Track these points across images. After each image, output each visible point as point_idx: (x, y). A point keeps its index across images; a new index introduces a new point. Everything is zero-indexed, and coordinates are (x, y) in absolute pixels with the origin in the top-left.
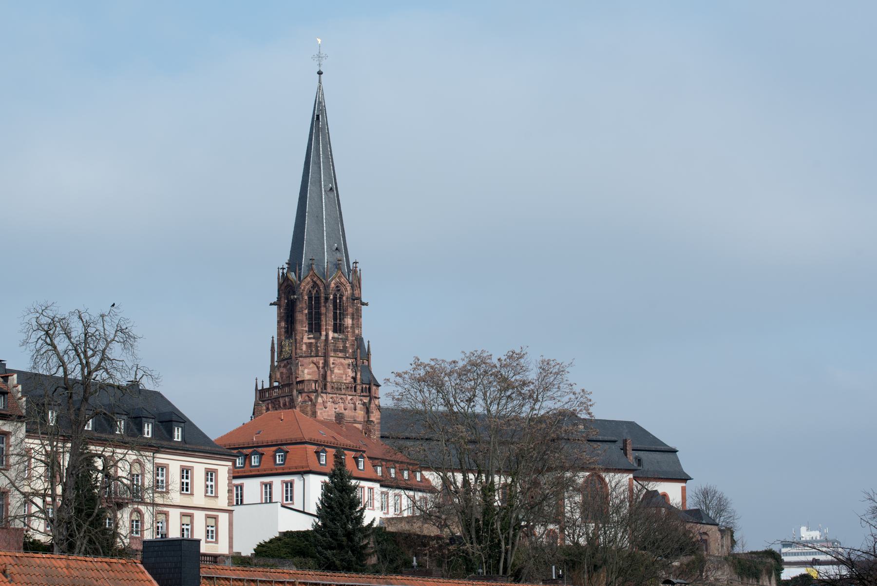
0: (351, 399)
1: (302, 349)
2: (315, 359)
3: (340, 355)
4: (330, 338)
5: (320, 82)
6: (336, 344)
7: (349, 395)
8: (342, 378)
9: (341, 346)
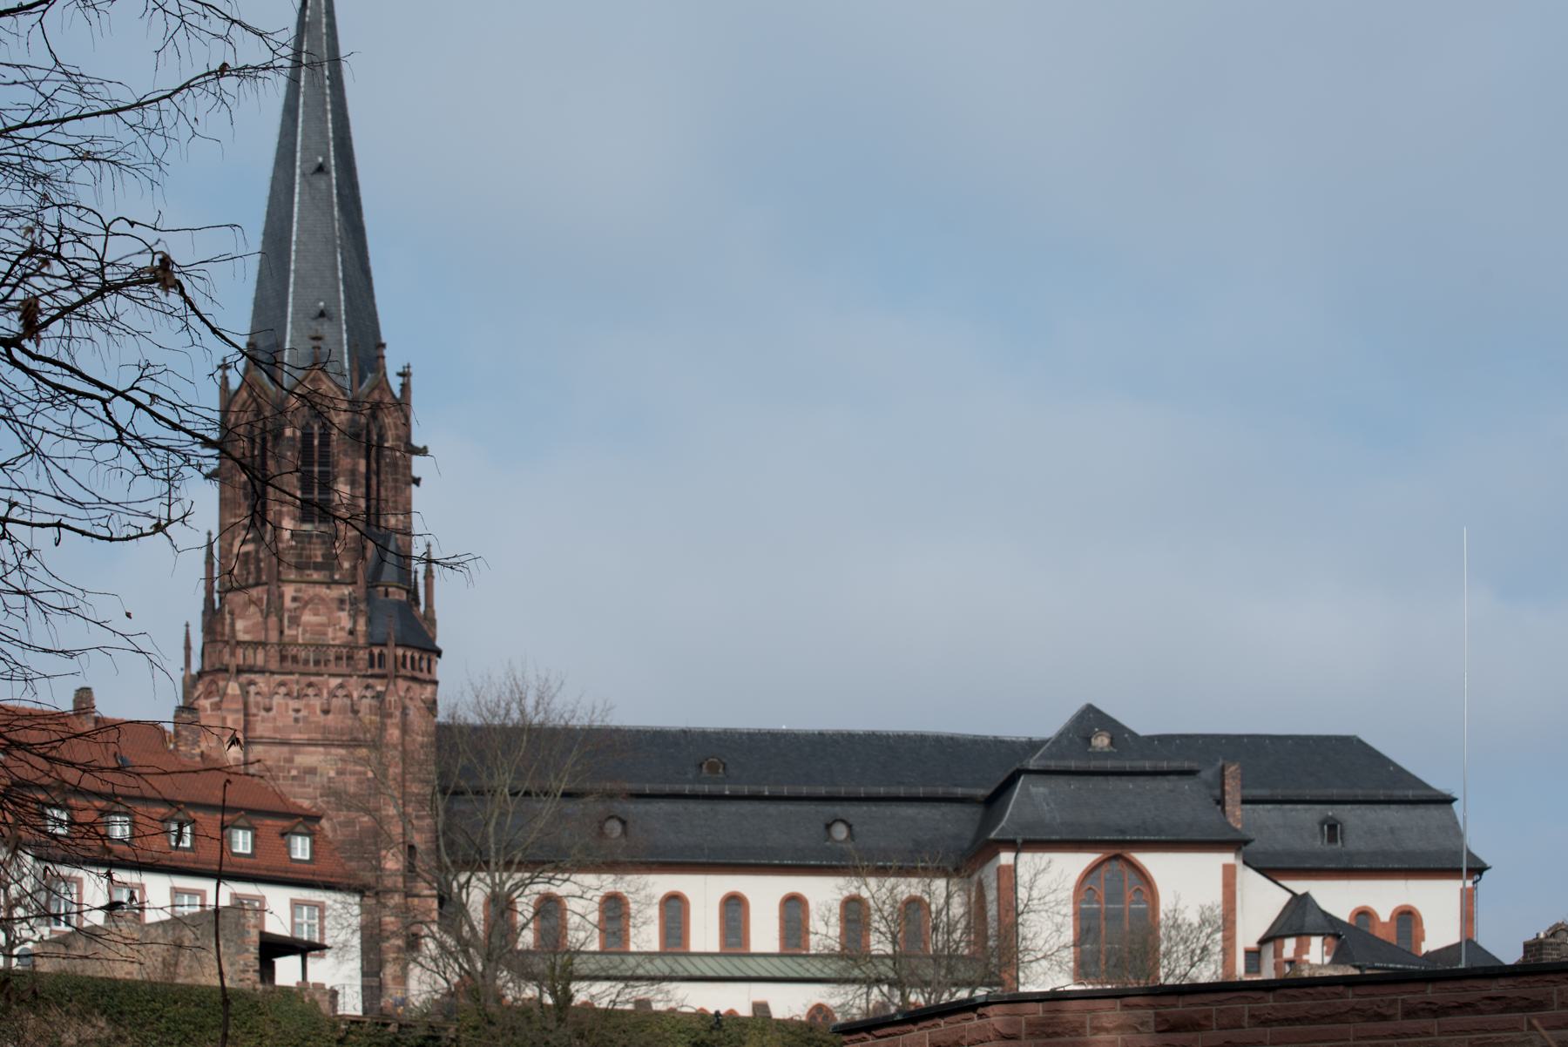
0: (341, 686)
2: (255, 593)
3: (316, 576)
4: (287, 535)
6: (302, 549)
8: (325, 634)
9: (318, 555)
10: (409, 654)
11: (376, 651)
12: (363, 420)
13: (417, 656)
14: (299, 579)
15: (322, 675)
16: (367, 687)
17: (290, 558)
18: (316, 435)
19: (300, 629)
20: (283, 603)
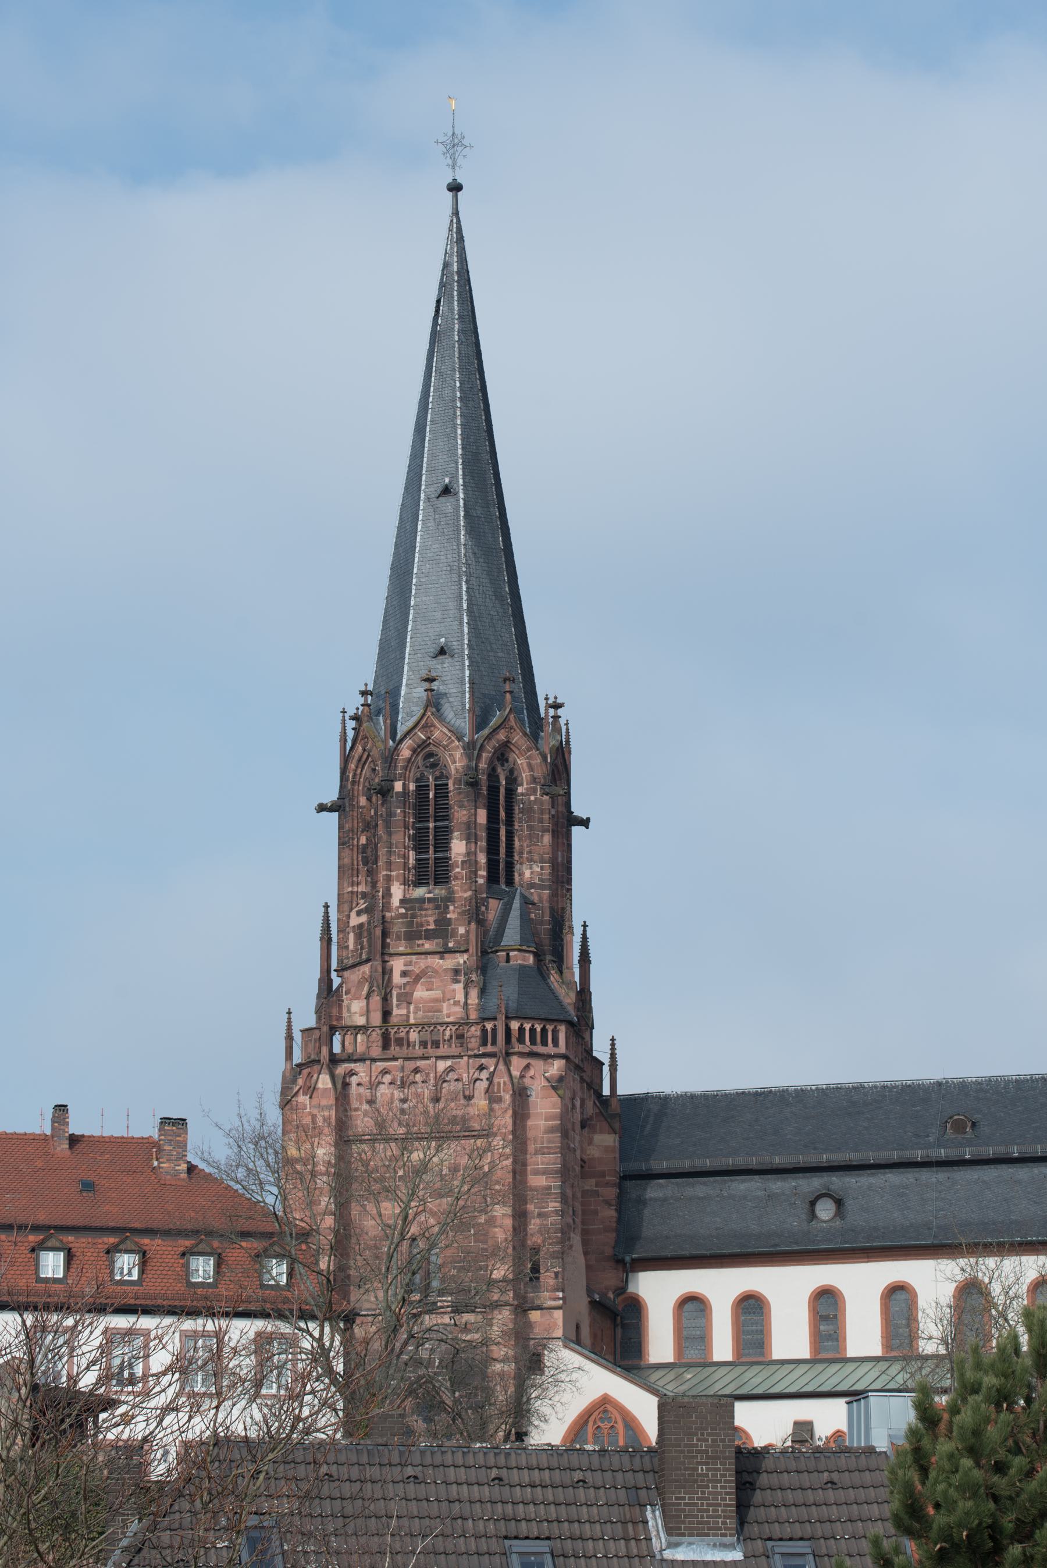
0: (451, 1069)
1: (347, 947)
2: (366, 969)
3: (428, 946)
4: (395, 901)
5: (456, 213)
6: (413, 916)
7: (438, 1058)
8: (440, 1011)
10: (527, 1026)
11: (489, 1026)
12: (482, 765)
13: (538, 1028)
14: (409, 951)
15: (427, 1058)
16: (481, 1068)
17: (398, 928)
18: (432, 787)
19: (412, 1007)
20: (390, 979)
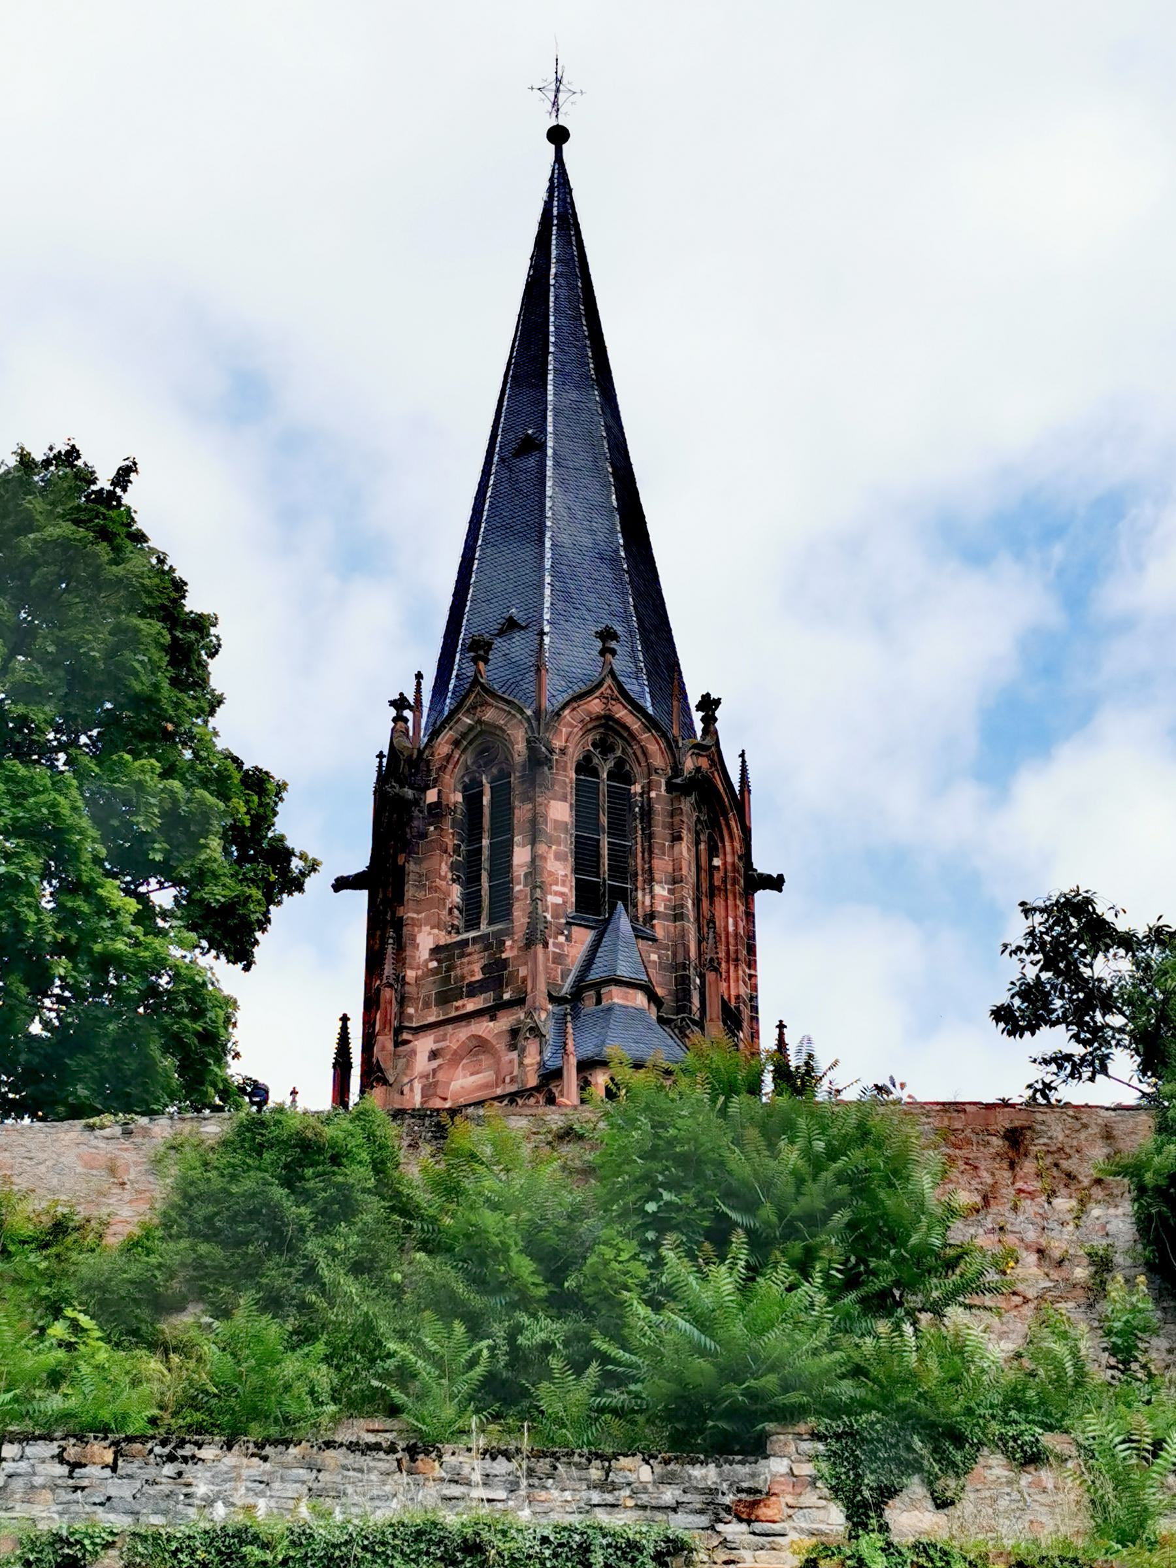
3: (471, 1005)
6: (449, 969)
9: (473, 968)
